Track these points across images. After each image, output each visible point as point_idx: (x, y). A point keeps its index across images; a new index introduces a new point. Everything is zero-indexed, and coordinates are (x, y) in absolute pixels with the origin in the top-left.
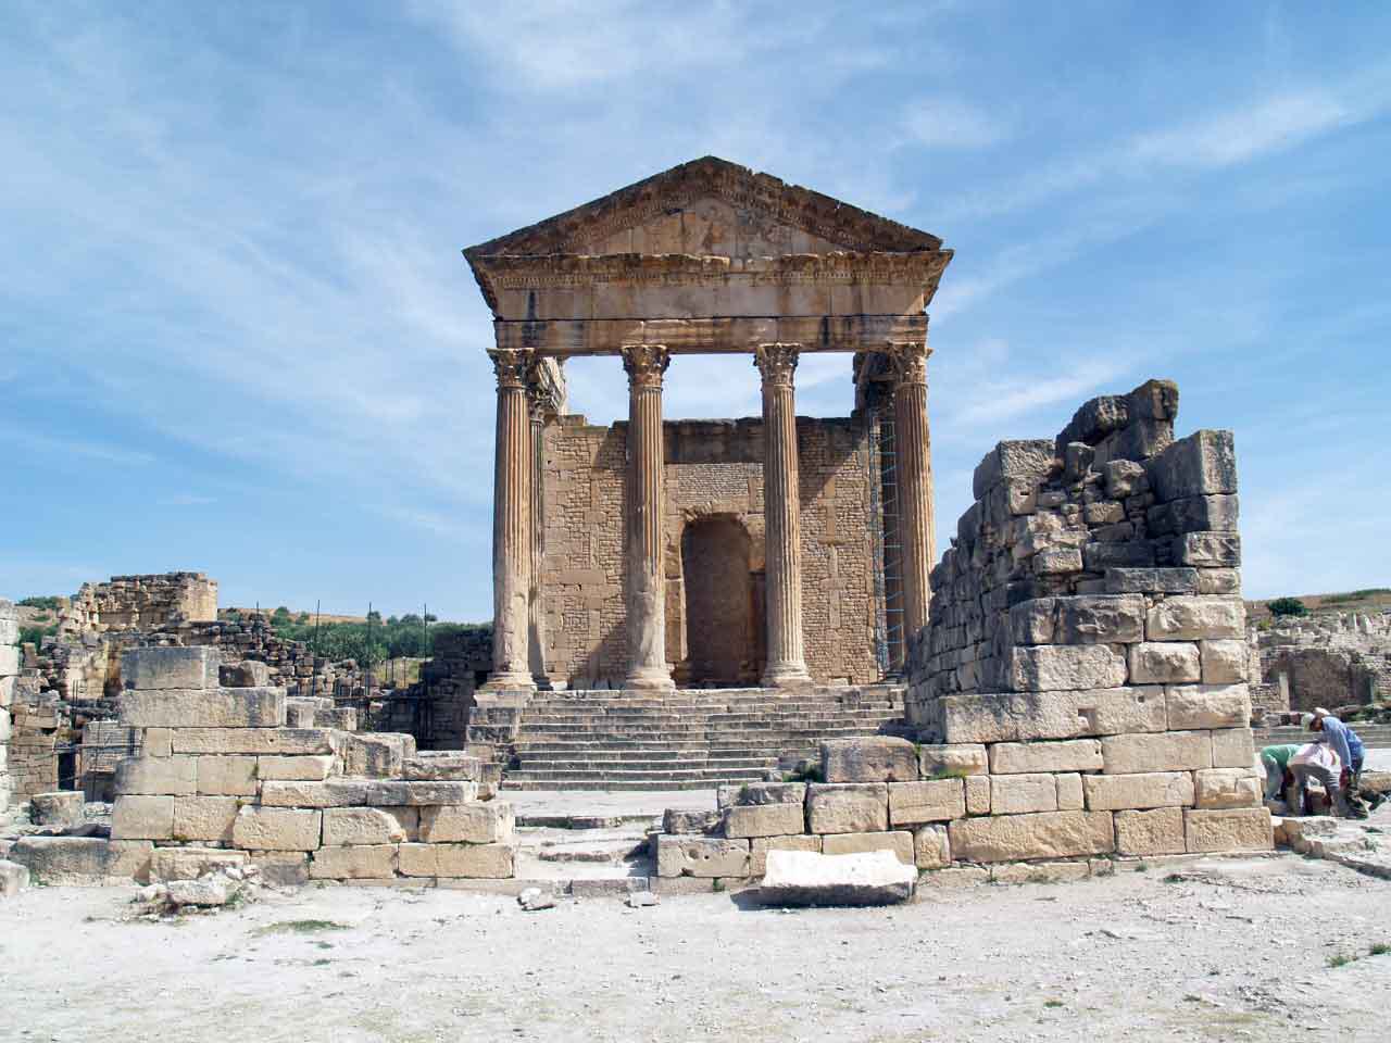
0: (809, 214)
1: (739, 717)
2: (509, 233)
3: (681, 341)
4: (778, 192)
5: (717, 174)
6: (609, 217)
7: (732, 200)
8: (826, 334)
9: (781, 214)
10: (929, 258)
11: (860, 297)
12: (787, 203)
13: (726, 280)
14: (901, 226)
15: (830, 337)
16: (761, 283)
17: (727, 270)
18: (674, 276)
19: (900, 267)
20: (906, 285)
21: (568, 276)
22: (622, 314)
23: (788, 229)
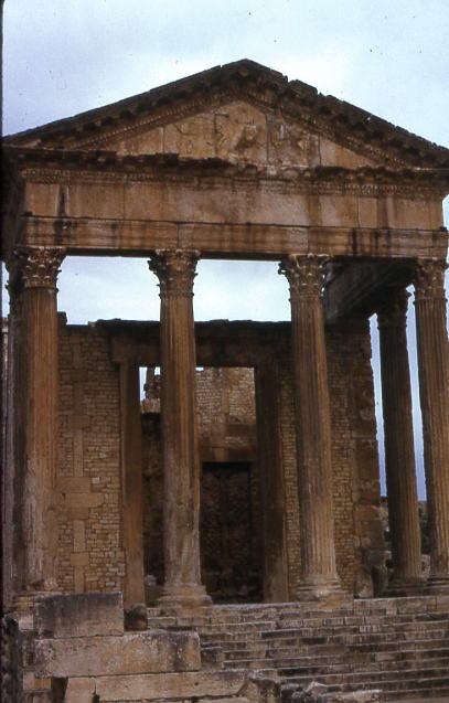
0: (338, 123)
1: (292, 633)
3: (216, 245)
8: (354, 246)
9: (310, 123)
15: (359, 249)
18: (207, 179)
21: (100, 173)
22: (155, 216)
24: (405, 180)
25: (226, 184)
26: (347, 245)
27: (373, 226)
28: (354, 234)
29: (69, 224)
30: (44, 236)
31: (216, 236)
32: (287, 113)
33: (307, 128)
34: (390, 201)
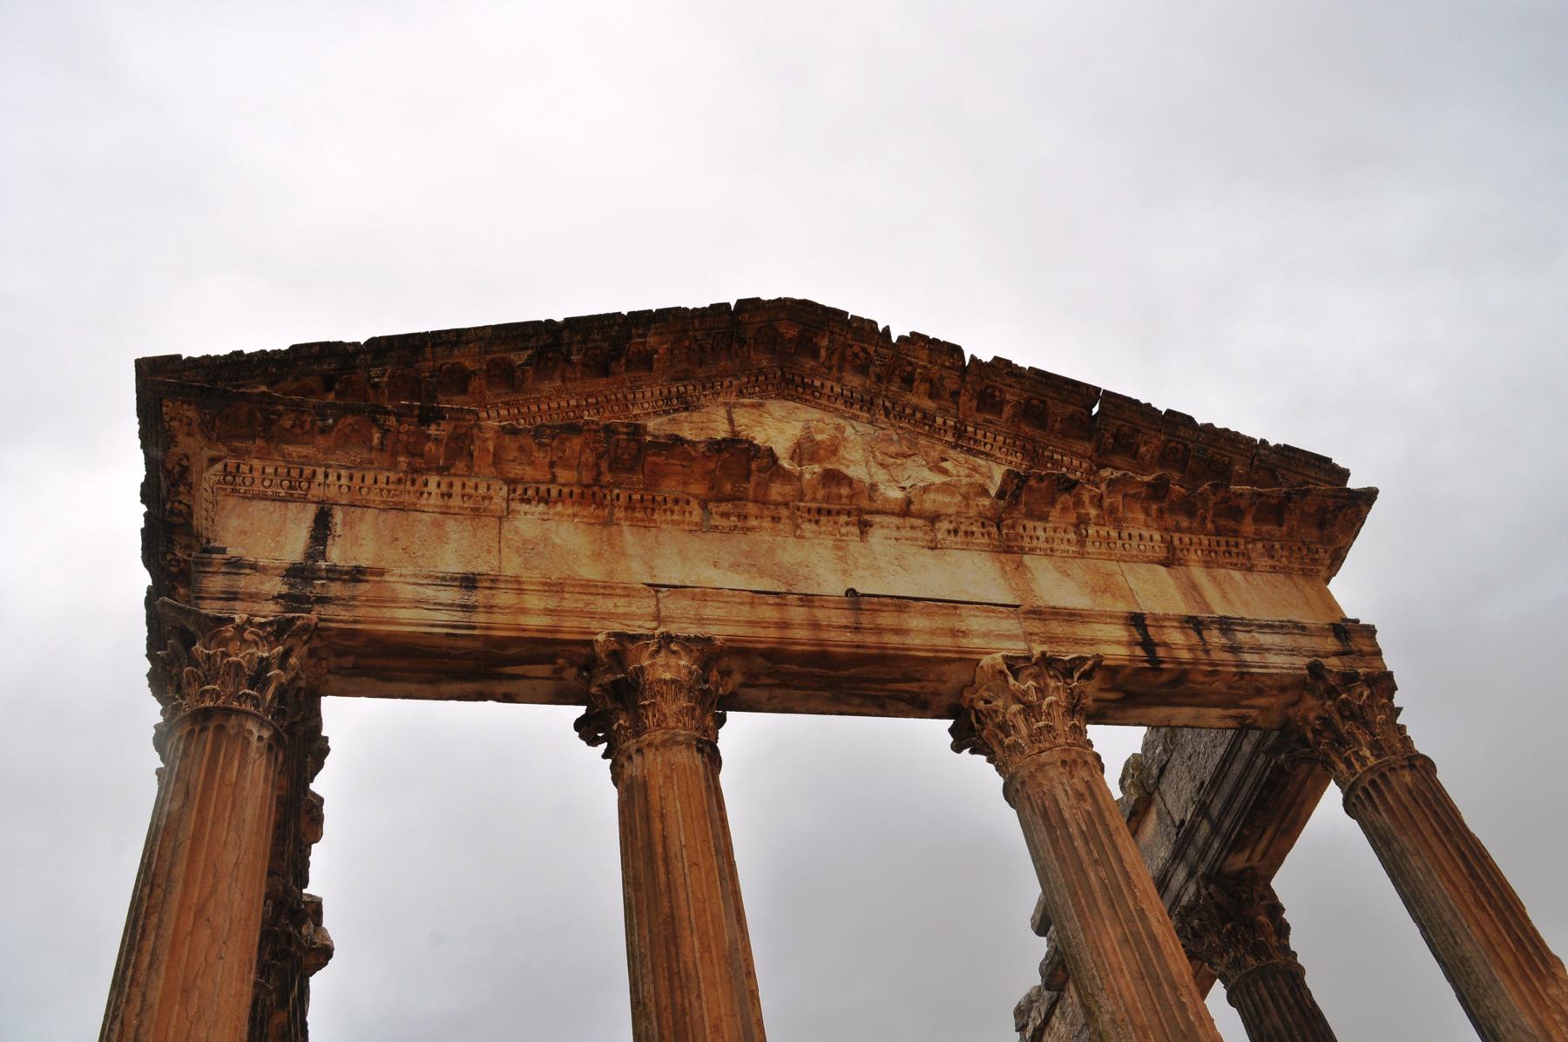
0: (1023, 426)
2: (285, 347)
3: (773, 633)
4: (951, 383)
5: (806, 346)
6: (547, 387)
7: (839, 405)
8: (1148, 644)
10: (1330, 503)
11: (1194, 587)
12: (975, 403)
13: (864, 527)
14: (1250, 441)
15: (1161, 652)
16: (952, 538)
17: (865, 504)
18: (725, 507)
19: (1266, 528)
20: (1287, 572)
21: (433, 480)
23: (980, 461)
24: (1222, 522)
25: (776, 519)
26: (1131, 644)
27: (1180, 606)
28: (1136, 621)
29: (334, 573)
30: (253, 597)
31: (768, 613)
32: (901, 416)
33: (955, 447)
34: (1198, 573)
